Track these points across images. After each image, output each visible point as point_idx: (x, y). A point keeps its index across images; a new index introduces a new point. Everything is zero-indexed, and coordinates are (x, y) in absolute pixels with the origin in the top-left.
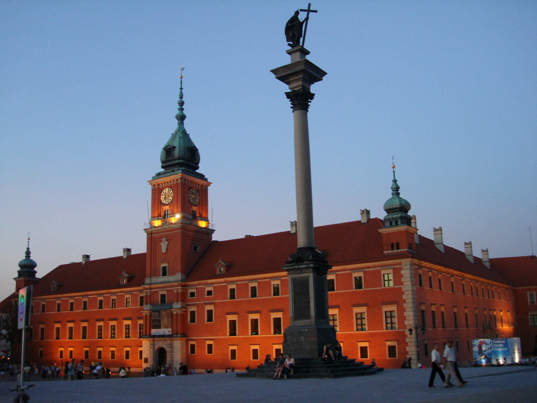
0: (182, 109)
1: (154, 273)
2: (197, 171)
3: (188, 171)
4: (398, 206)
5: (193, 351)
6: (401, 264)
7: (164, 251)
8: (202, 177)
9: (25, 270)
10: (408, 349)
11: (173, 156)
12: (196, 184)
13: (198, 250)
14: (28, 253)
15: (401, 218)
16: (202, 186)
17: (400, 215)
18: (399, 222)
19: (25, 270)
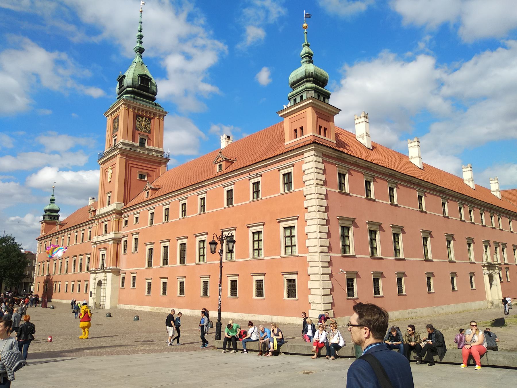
0: (141, 43)
1: (103, 206)
2: (155, 102)
3: (135, 98)
4: (303, 75)
5: (123, 285)
6: (302, 153)
7: (109, 180)
8: (156, 105)
9: (47, 214)
10: (310, 284)
11: (123, 86)
12: (146, 112)
13: (146, 179)
14: (53, 201)
15: (307, 89)
16: (155, 114)
17: (304, 87)
18: (304, 98)
19: (47, 214)
